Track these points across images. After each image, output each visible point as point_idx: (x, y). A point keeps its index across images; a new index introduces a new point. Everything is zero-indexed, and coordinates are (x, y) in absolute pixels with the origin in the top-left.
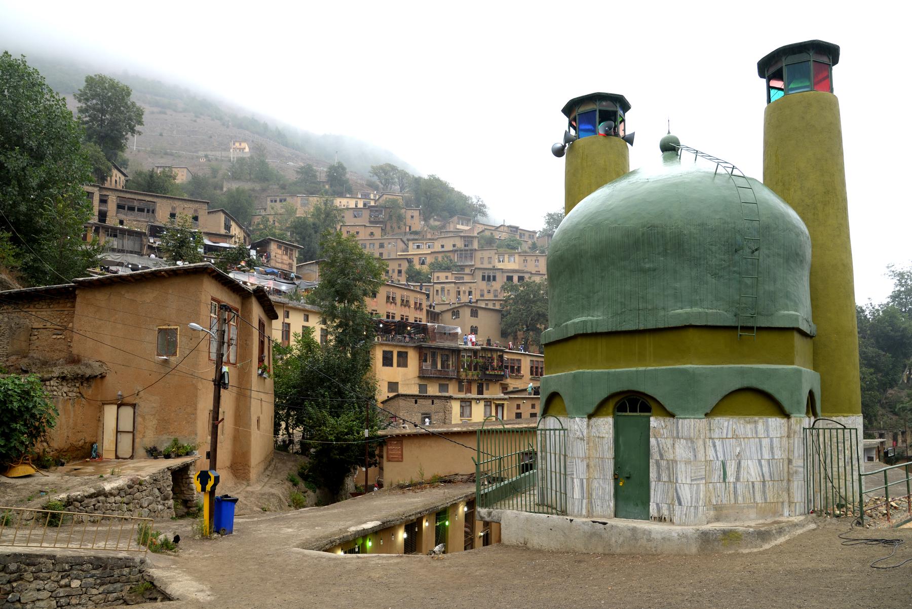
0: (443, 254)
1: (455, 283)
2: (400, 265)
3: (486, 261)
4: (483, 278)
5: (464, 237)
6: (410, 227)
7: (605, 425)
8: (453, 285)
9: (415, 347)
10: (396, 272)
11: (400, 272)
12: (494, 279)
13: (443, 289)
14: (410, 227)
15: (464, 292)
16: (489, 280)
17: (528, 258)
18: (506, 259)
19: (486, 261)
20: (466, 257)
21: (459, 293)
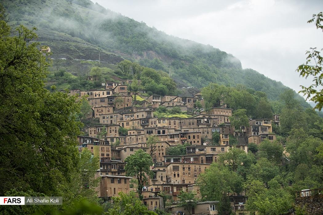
0: (136, 121)
2: (116, 128)
4: (147, 133)
6: (127, 104)
8: (135, 136)
10: (114, 131)
11: (116, 130)
12: (152, 132)
13: (131, 138)
14: (127, 104)
15: (140, 139)
16: (150, 133)
18: (162, 122)
21: (137, 139)
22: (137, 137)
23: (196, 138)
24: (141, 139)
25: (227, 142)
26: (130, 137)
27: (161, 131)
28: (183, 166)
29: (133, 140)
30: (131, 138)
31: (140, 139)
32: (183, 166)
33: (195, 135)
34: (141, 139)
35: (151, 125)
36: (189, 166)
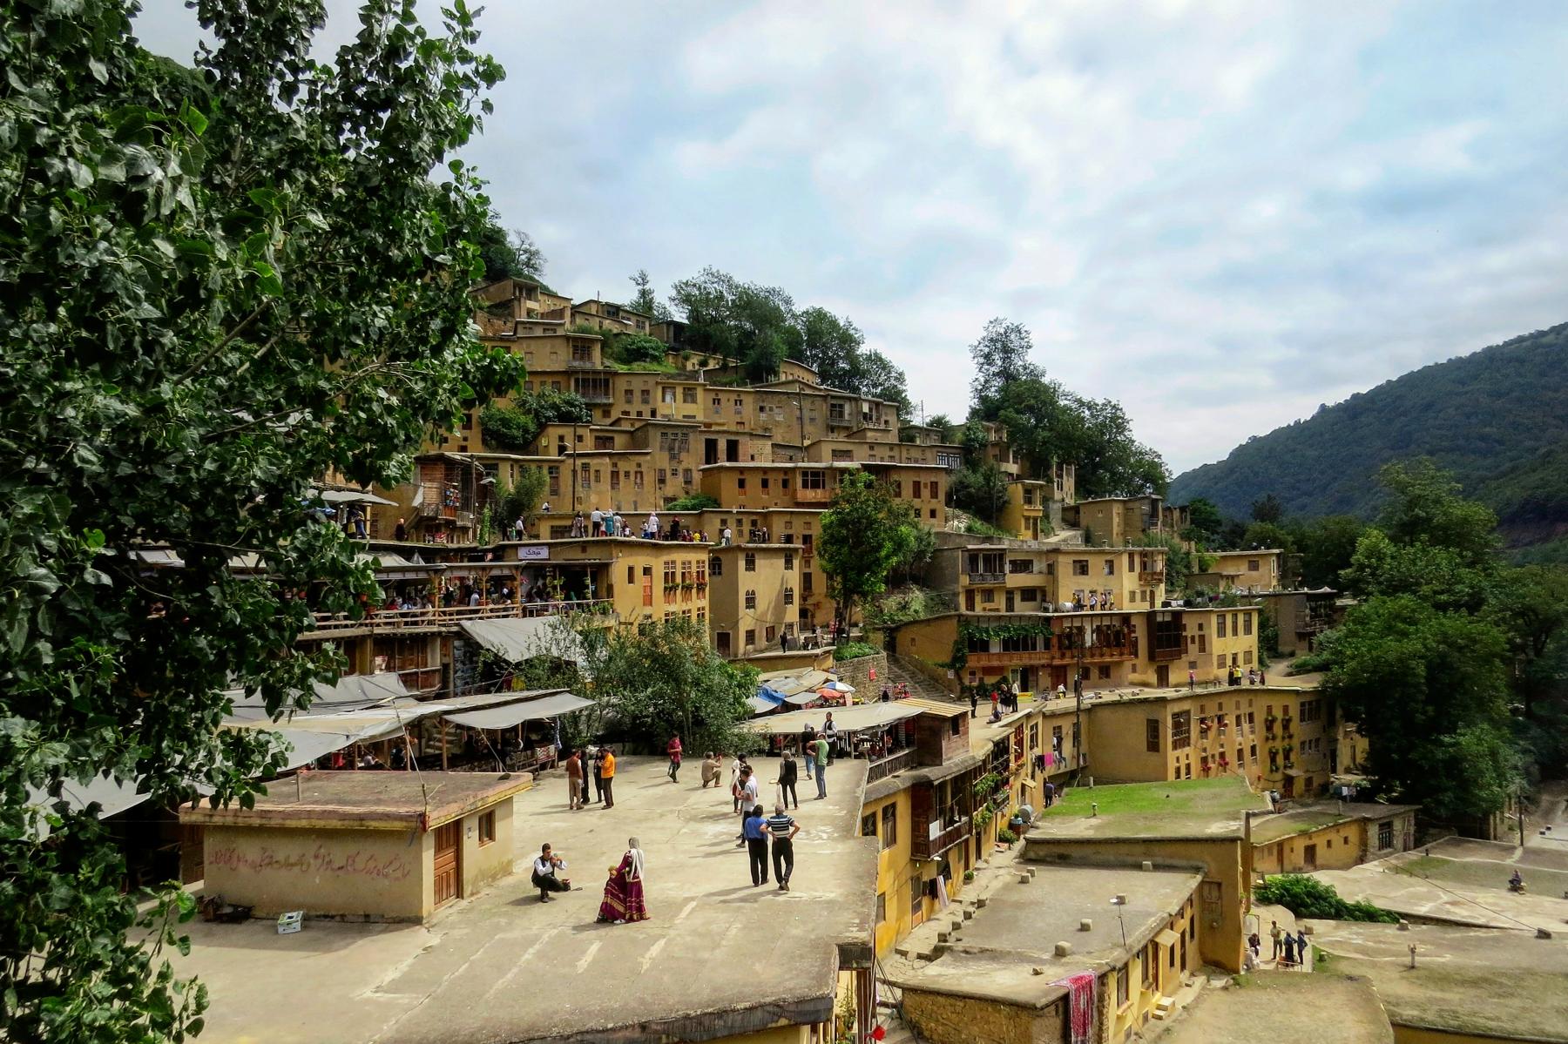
1: (609, 455)
3: (637, 396)
5: (575, 339)
13: (585, 467)
15: (627, 474)
19: (637, 396)
20: (595, 387)
22: (615, 465)
23: (926, 493)
24: (632, 477)
25: (1035, 519)
26: (586, 460)
27: (722, 445)
28: (1202, 709)
29: (598, 479)
30: (585, 467)
31: (627, 474)
32: (1202, 709)
33: (925, 479)
34: (632, 477)
35: (627, 408)
36: (1220, 706)
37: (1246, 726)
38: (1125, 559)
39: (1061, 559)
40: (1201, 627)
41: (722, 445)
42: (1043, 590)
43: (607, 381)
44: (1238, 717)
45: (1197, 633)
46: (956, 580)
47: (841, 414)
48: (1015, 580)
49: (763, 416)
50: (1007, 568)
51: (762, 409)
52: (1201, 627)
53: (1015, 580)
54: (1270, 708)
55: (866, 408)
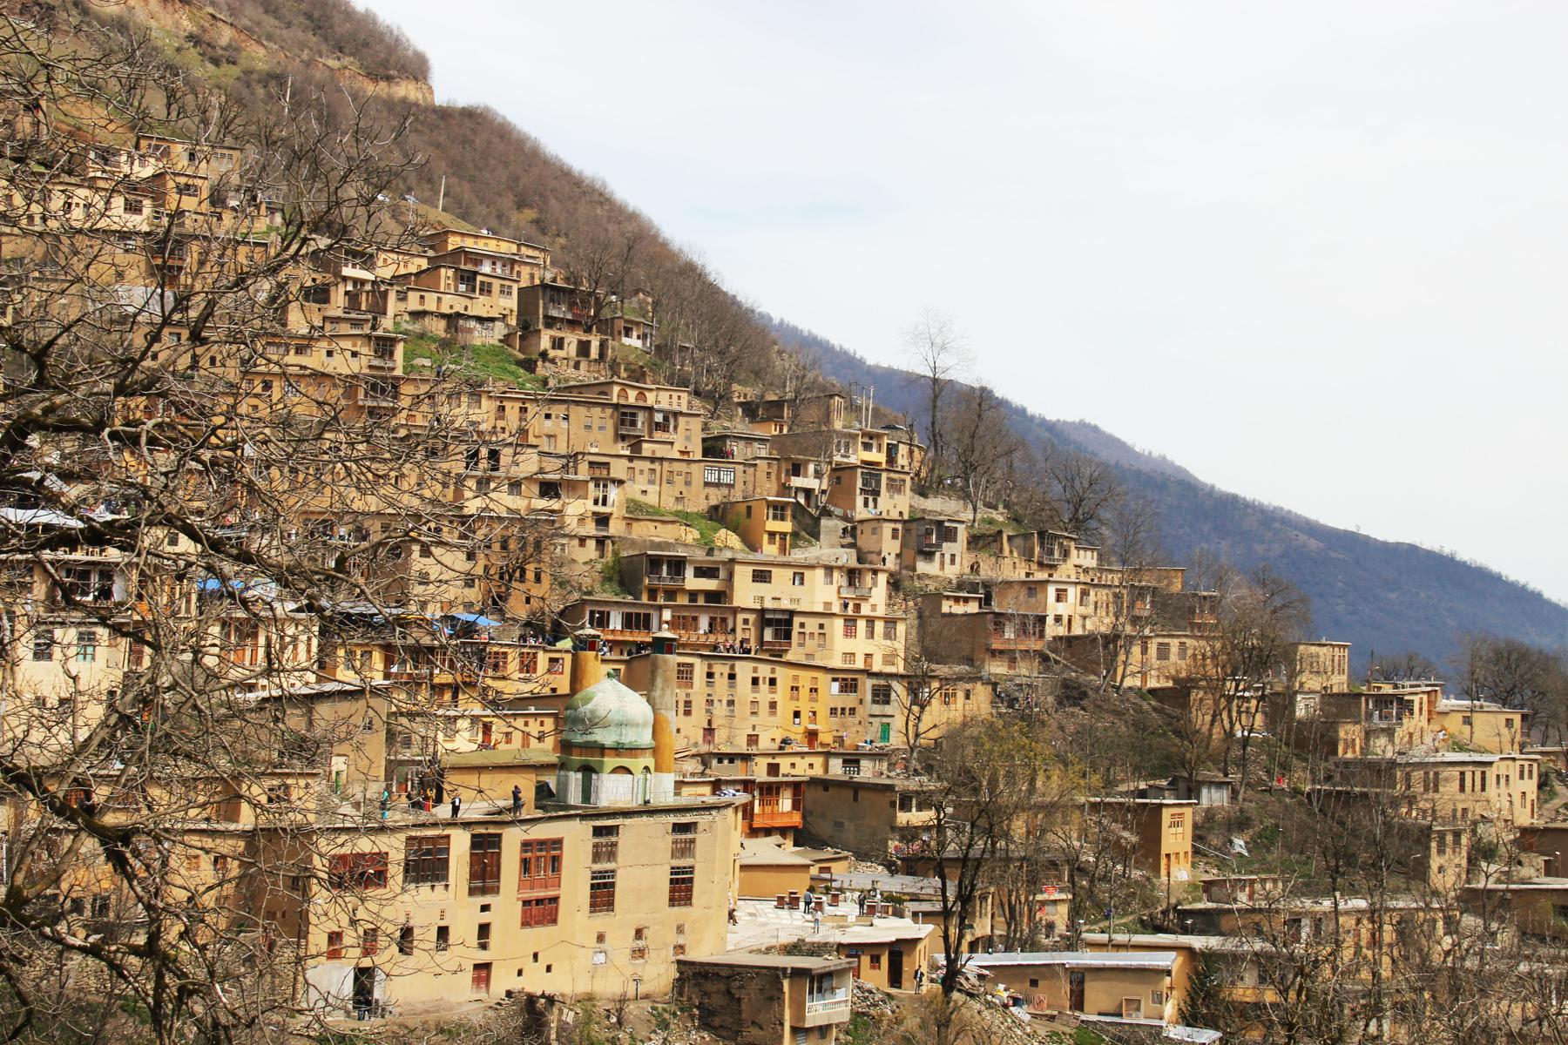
7: (579, 775)
9: (380, 646)
17: (508, 405)
25: (783, 535)
28: (710, 666)
36: (732, 667)
37: (764, 687)
38: (820, 573)
39: (738, 568)
40: (821, 626)
41: (484, 452)
42: (724, 593)
43: (395, 387)
44: (755, 681)
45: (817, 631)
46: (641, 581)
47: (633, 423)
48: (692, 582)
49: (548, 423)
50: (689, 572)
51: (548, 416)
52: (821, 626)
53: (692, 582)
54: (796, 678)
55: (659, 418)
